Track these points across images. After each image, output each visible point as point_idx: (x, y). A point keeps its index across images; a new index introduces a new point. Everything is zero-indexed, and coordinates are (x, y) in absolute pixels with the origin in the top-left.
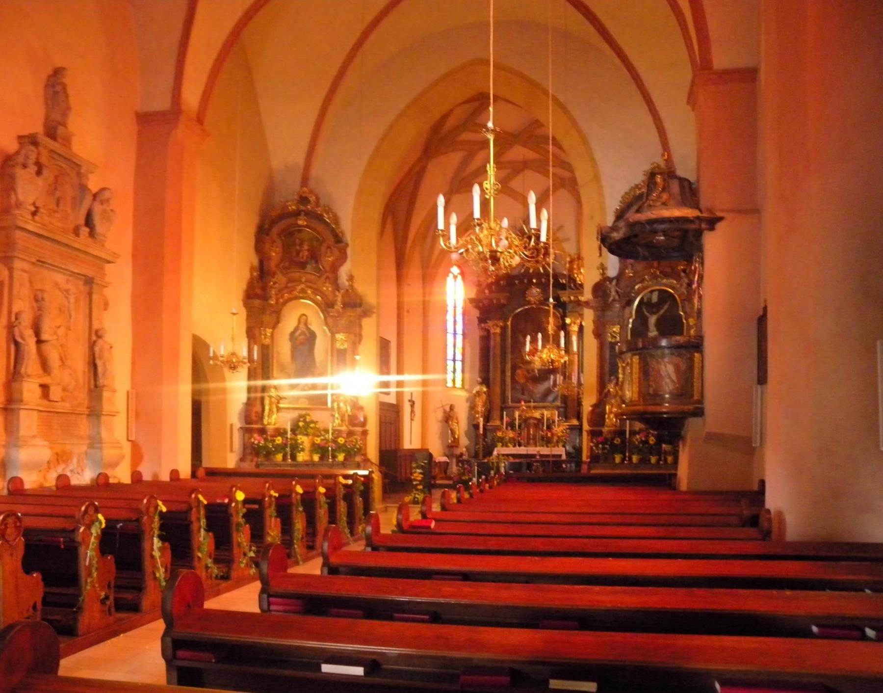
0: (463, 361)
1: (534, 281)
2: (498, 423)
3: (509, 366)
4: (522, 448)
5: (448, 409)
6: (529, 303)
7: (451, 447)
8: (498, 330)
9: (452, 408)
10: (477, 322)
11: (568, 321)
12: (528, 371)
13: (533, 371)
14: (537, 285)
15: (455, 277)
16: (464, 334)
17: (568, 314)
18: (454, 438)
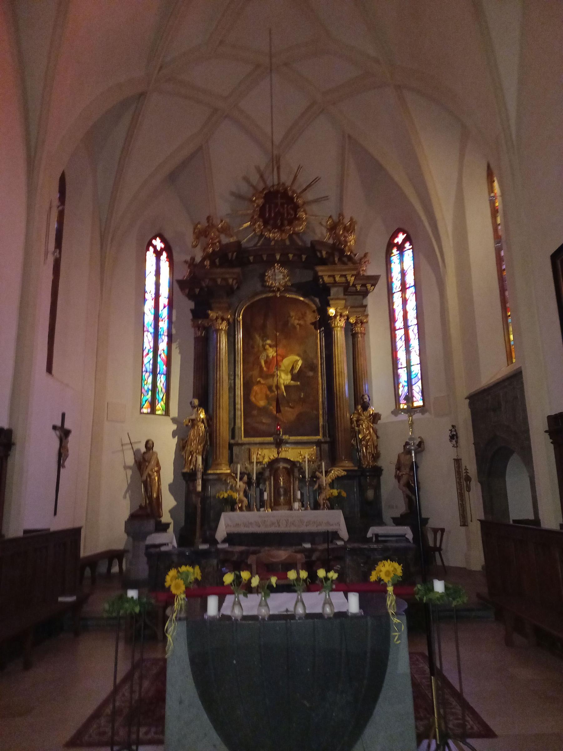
0: (168, 375)
1: (278, 257)
2: (225, 470)
3: (240, 382)
4: (267, 512)
5: (143, 450)
6: (270, 289)
7: (145, 514)
8: (224, 326)
9: (149, 446)
10: (190, 316)
11: (332, 311)
12: (270, 388)
13: (278, 387)
14: (284, 263)
15: (158, 254)
16: (170, 336)
17: (331, 302)
18: (150, 497)
